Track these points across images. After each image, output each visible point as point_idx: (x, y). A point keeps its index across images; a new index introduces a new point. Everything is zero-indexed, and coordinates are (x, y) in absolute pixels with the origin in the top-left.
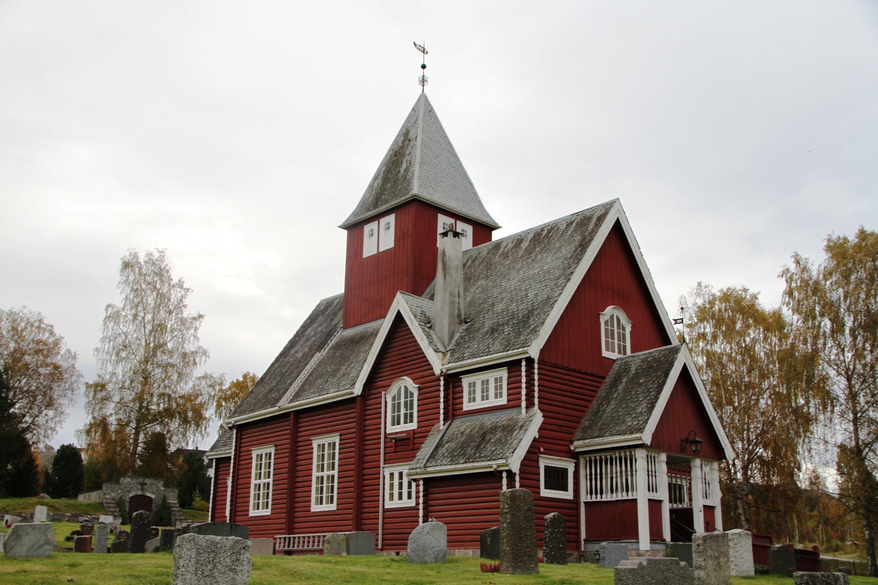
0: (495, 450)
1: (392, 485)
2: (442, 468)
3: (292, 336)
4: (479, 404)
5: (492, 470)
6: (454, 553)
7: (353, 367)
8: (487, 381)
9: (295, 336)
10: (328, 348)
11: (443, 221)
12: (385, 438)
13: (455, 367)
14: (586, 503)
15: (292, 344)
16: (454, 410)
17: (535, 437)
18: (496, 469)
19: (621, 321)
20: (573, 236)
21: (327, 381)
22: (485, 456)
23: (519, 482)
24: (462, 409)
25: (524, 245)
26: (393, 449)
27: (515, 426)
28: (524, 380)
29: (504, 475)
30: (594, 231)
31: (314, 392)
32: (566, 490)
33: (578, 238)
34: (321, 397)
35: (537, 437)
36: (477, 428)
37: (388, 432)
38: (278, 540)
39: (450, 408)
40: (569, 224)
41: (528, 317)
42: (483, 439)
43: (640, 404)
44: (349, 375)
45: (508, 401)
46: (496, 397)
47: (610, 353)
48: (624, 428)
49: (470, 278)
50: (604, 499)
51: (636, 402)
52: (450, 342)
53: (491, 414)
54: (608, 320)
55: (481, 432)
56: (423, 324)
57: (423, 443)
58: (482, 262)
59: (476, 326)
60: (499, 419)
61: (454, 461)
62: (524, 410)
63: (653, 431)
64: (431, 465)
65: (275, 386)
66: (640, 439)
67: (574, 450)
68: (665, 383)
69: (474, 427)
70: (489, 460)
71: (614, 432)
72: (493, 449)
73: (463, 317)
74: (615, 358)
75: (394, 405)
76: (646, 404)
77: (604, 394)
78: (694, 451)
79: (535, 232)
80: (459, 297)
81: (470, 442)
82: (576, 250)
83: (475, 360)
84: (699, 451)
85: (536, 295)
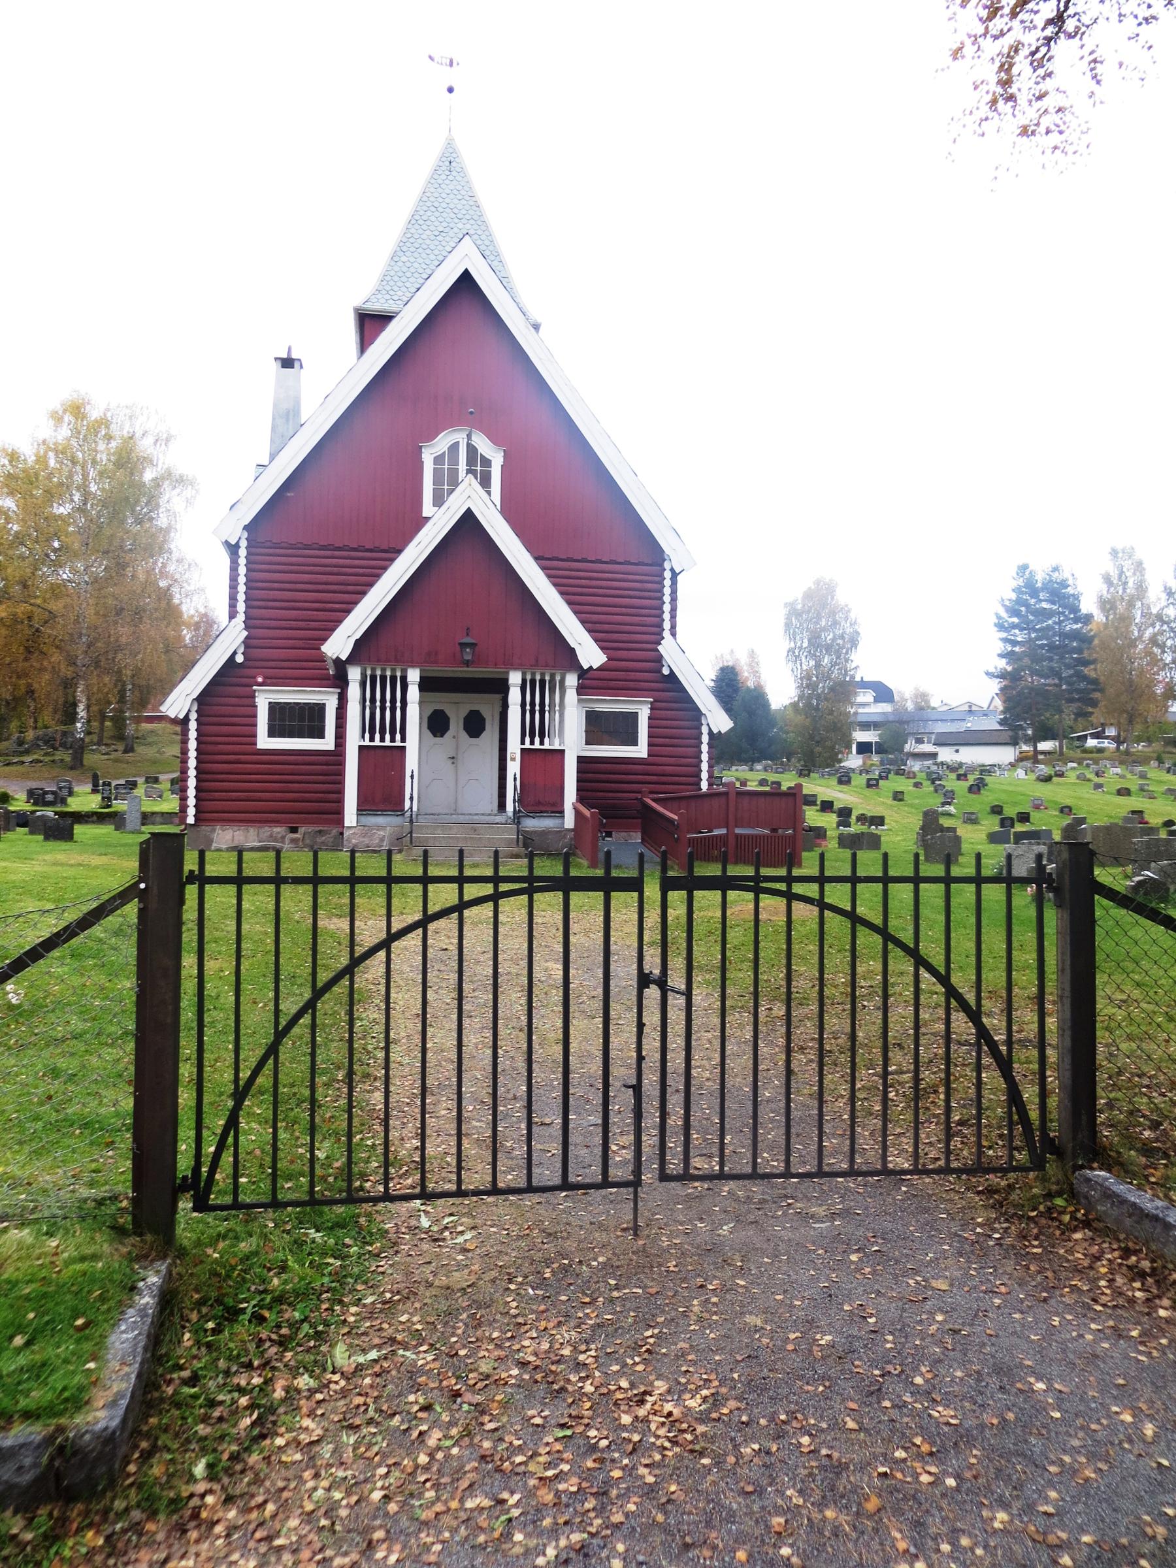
32: (323, 737)
35: (240, 659)
63: (358, 635)
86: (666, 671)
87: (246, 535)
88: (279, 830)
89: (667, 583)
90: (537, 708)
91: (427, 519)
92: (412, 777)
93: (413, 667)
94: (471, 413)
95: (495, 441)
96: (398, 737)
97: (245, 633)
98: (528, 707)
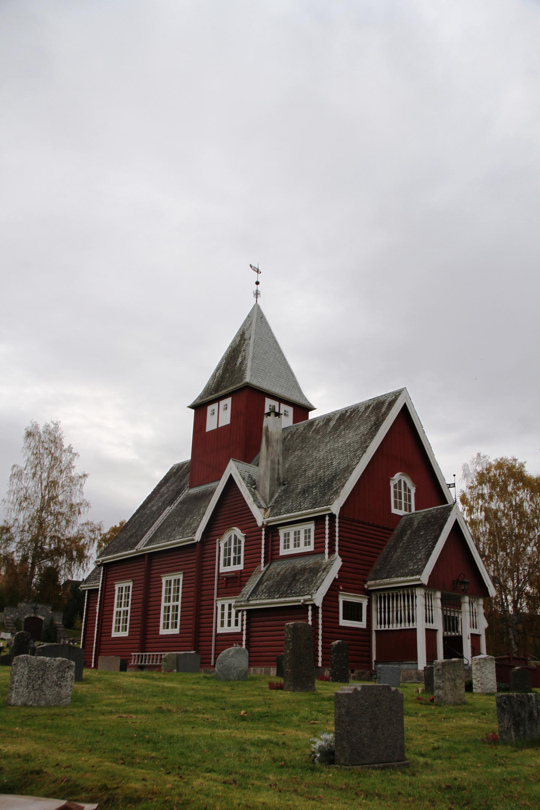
0: (304, 587)
1: (223, 615)
2: (261, 601)
3: (150, 493)
4: (292, 550)
5: (300, 604)
6: (270, 670)
7: (196, 518)
8: (299, 532)
9: (153, 493)
10: (176, 503)
11: (269, 403)
12: (219, 576)
13: (274, 520)
14: (376, 631)
15: (150, 499)
16: (272, 555)
17: (335, 578)
18: (303, 603)
20: (369, 417)
21: (174, 530)
22: (295, 593)
23: (322, 613)
24: (279, 554)
25: (332, 424)
26: (224, 585)
27: (319, 568)
28: (327, 531)
29: (310, 608)
30: (386, 414)
31: (164, 539)
32: (361, 621)
33: (373, 419)
34: (169, 543)
35: (337, 577)
36: (290, 570)
37: (221, 571)
38: (133, 657)
39: (270, 553)
40: (367, 408)
41: (332, 482)
42: (294, 579)
43: (420, 552)
44: (192, 525)
45: (315, 548)
46: (305, 545)
47: (398, 510)
48: (407, 571)
49: (289, 449)
50: (391, 628)
51: (416, 550)
52: (270, 500)
53: (302, 559)
55: (293, 573)
56: (250, 485)
57: (247, 581)
58: (299, 437)
59: (292, 487)
60: (308, 563)
61: (270, 597)
62: (327, 556)
63: (429, 574)
64: (253, 598)
65: (135, 533)
66: (419, 580)
67: (367, 588)
68: (440, 535)
69: (288, 569)
70: (298, 596)
71: (399, 574)
72: (301, 587)
73: (282, 480)
74: (402, 515)
75: (225, 550)
76: (424, 552)
77: (392, 544)
78: (463, 590)
79: (340, 413)
80: (279, 464)
81: (284, 581)
82: (370, 429)
83: (289, 515)
84: (467, 590)
85: (339, 463)
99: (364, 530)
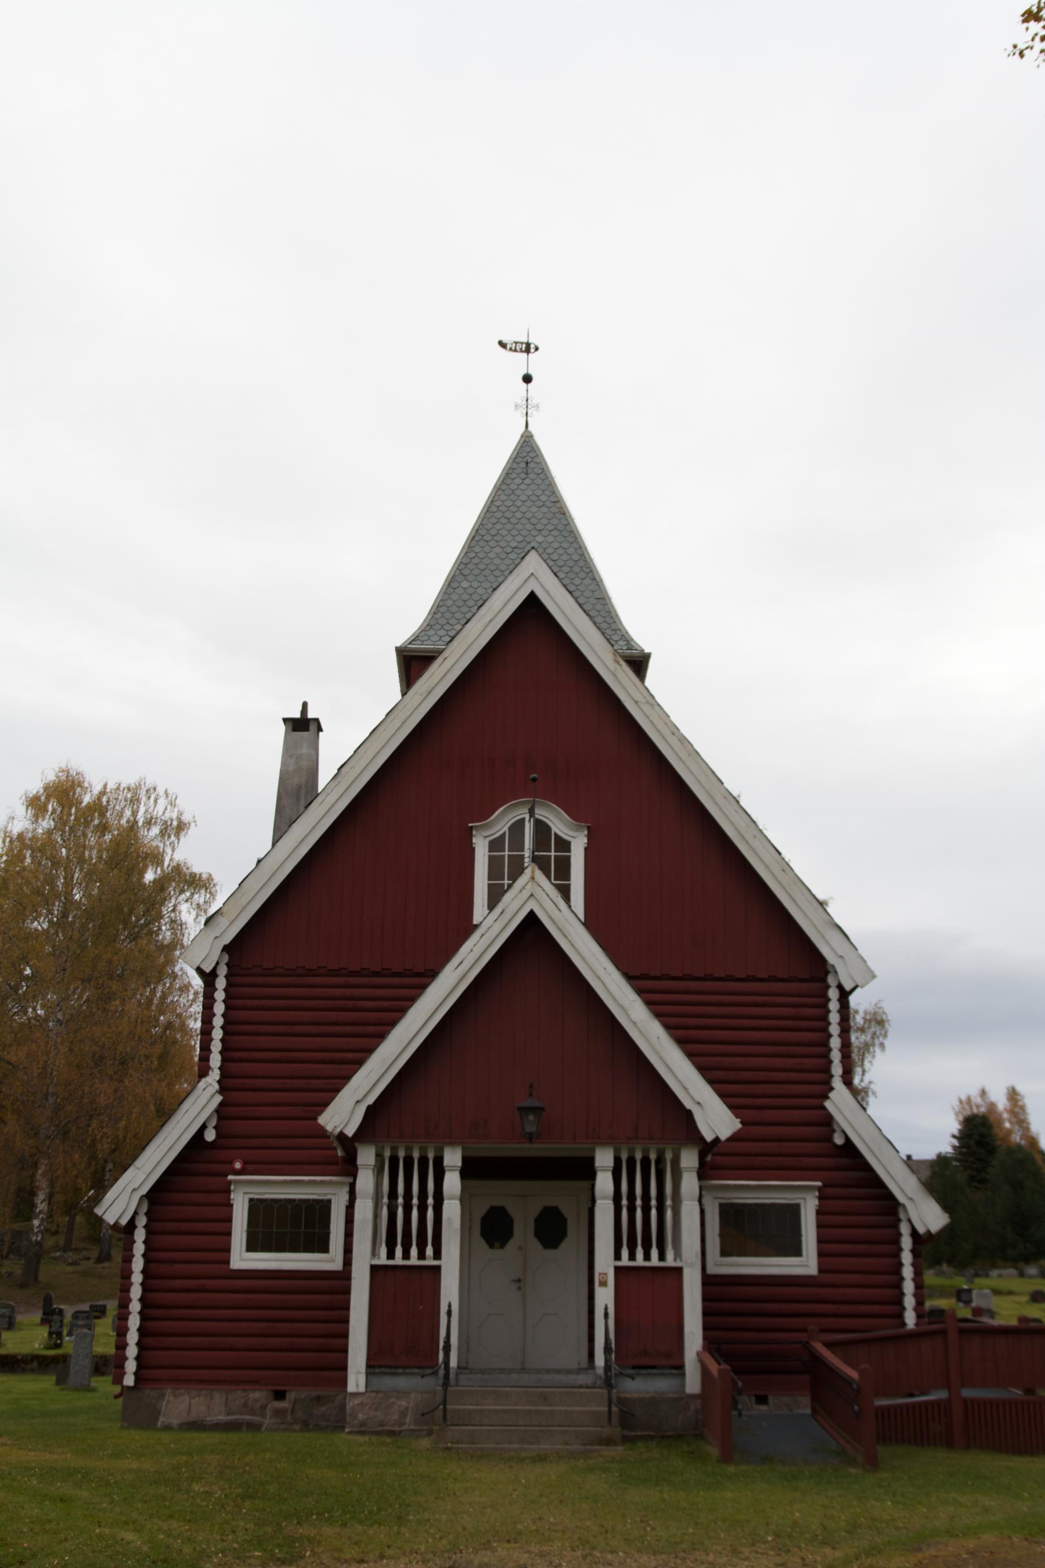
19: (554, 829)
32: (324, 1248)
35: (210, 1136)
54: (504, 834)
63: (371, 1100)
86: (839, 1140)
87: (226, 958)
88: (258, 1395)
89: (834, 1006)
90: (639, 1202)
91: (476, 926)
92: (449, 1313)
93: (452, 1144)
94: (534, 780)
95: (576, 815)
96: (429, 1251)
97: (219, 1098)
98: (625, 1202)
99: (348, 992)
